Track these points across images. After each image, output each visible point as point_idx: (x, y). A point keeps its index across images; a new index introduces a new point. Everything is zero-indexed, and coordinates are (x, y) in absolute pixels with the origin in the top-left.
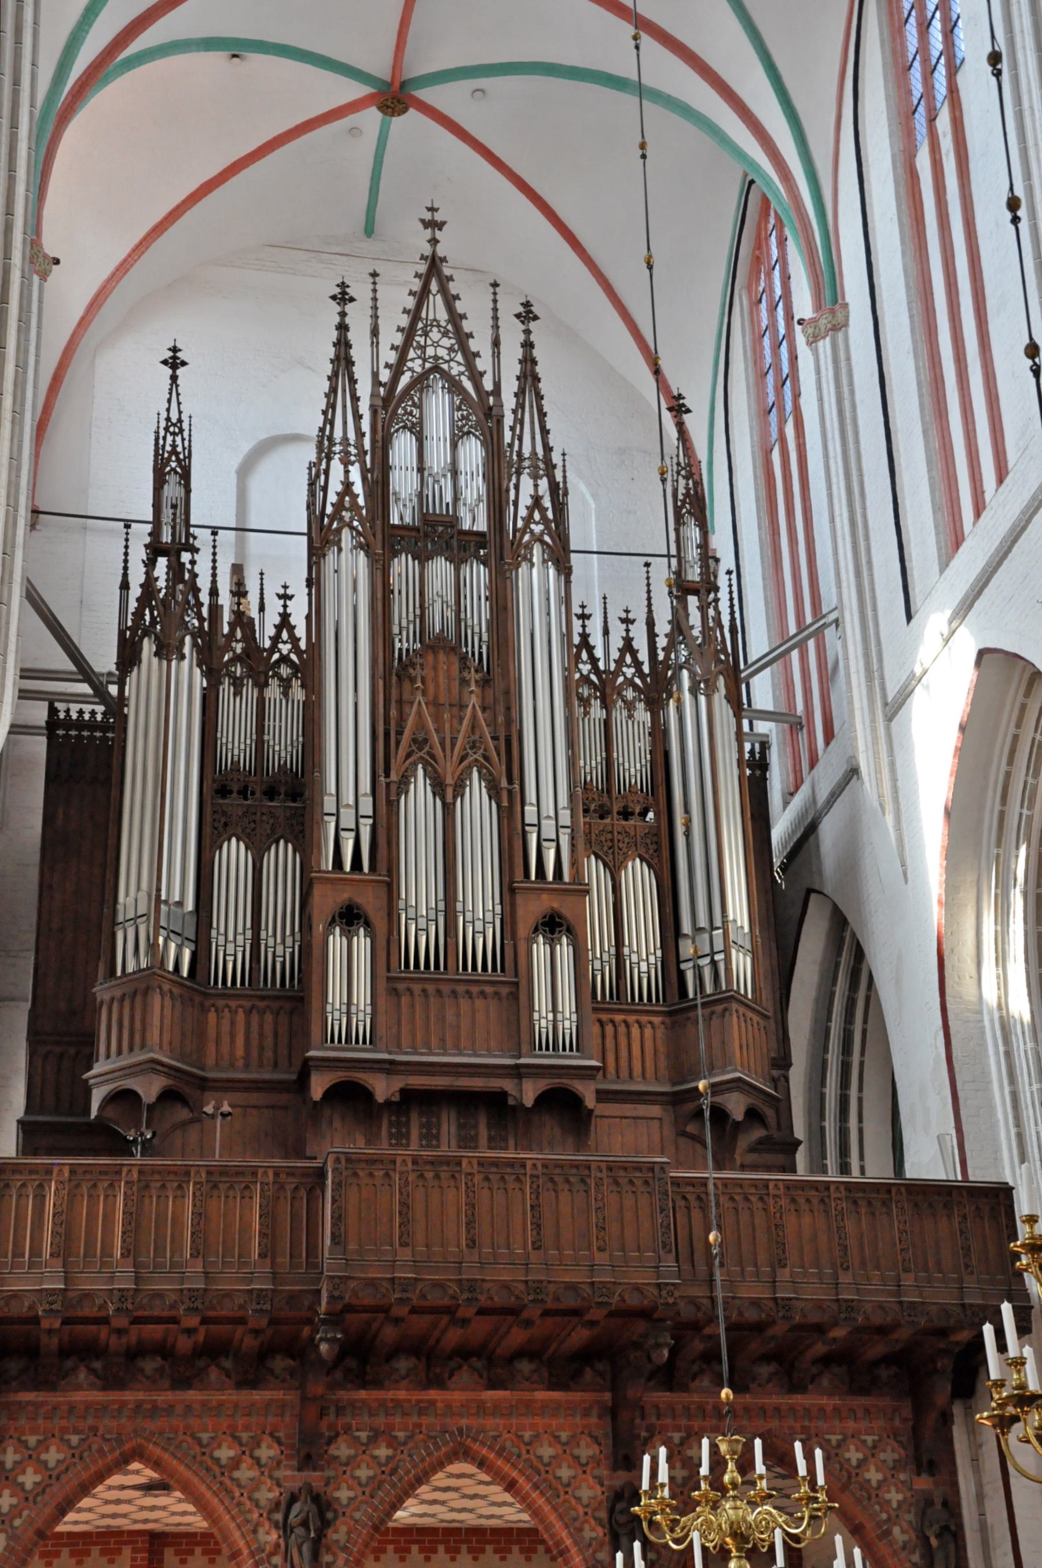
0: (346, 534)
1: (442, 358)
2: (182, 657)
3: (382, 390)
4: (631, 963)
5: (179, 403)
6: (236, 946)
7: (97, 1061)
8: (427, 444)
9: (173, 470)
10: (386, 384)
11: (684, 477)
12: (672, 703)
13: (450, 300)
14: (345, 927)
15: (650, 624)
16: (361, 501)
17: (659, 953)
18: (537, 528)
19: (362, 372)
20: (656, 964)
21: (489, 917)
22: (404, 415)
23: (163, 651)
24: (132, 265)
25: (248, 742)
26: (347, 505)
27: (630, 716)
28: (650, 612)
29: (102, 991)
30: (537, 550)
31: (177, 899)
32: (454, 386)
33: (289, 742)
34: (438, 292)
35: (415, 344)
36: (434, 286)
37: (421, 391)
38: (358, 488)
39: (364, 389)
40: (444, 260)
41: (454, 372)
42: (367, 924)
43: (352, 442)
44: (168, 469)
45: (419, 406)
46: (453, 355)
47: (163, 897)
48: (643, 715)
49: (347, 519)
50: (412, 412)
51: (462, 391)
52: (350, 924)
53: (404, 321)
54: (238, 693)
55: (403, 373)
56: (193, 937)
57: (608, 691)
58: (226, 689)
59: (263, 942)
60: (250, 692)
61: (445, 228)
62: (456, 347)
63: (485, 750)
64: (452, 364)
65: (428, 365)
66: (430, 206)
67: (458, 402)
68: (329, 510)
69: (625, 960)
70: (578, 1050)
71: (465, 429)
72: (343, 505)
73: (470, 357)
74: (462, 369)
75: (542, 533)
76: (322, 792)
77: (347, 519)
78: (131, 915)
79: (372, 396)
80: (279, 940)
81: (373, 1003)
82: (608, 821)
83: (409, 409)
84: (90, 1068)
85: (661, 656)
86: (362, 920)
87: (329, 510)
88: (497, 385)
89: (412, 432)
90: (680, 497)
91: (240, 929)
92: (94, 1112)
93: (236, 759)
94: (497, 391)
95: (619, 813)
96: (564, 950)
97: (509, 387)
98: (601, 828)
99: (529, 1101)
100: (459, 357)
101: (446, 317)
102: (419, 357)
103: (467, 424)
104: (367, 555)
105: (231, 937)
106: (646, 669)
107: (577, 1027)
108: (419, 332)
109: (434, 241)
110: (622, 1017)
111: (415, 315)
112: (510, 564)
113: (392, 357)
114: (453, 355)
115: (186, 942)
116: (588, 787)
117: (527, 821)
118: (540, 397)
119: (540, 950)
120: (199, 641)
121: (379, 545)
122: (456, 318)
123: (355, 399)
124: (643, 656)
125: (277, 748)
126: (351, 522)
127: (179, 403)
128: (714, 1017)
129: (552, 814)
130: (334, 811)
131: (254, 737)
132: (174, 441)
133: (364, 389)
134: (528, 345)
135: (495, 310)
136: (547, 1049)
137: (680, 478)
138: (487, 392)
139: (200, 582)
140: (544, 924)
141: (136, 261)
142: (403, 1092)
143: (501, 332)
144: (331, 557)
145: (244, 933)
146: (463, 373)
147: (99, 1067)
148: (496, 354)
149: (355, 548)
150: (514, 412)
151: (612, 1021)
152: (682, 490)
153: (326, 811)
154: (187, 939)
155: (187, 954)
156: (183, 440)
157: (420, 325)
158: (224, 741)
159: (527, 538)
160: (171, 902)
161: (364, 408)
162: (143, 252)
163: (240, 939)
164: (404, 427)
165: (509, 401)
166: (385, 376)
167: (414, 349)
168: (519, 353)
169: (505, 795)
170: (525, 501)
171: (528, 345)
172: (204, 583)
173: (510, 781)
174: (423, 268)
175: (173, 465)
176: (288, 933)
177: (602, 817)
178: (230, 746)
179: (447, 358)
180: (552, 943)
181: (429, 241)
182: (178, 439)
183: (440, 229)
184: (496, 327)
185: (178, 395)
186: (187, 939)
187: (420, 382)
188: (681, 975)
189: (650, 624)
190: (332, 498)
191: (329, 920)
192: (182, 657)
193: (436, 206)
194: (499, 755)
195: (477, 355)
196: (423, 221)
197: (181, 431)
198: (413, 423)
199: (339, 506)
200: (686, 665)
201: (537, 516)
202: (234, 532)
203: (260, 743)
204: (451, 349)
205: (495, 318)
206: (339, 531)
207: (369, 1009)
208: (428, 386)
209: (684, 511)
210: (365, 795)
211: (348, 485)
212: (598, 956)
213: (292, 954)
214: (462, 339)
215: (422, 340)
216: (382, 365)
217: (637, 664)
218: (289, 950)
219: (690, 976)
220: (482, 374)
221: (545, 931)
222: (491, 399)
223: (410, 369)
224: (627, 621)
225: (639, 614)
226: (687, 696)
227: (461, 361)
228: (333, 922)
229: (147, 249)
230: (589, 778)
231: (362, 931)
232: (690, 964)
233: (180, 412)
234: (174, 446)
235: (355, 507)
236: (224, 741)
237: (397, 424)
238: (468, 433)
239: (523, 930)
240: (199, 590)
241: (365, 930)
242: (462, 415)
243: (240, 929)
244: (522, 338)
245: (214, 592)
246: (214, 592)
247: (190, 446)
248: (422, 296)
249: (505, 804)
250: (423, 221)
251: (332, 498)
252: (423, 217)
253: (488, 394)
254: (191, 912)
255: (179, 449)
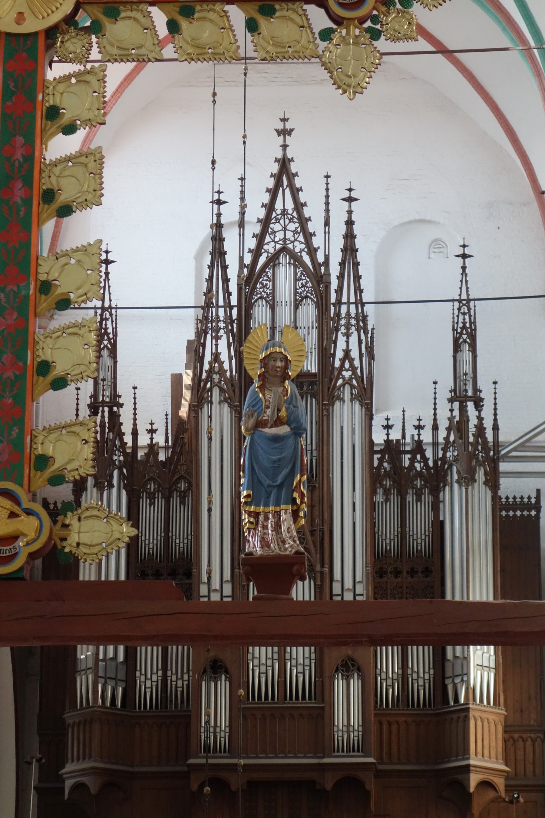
0: (216, 392)
1: (289, 240)
2: (113, 486)
3: (245, 270)
4: (412, 680)
5: (110, 294)
6: (152, 682)
7: (67, 763)
8: (277, 309)
9: (105, 346)
10: (248, 265)
11: (464, 314)
12: (447, 489)
13: (295, 192)
14: (213, 675)
15: (435, 428)
16: (226, 366)
17: (432, 672)
18: (347, 374)
19: (232, 260)
20: (429, 680)
21: (307, 662)
22: (261, 288)
23: (99, 486)
24: (112, 108)
25: (159, 538)
26: (216, 369)
27: (419, 499)
28: (435, 420)
29: (70, 717)
30: (347, 388)
31: (111, 656)
32: (296, 260)
33: (185, 537)
34: (287, 186)
35: (270, 230)
36: (285, 183)
37: (274, 266)
38: (224, 357)
39: (233, 273)
40: (292, 160)
41: (297, 250)
42: (227, 672)
43: (222, 318)
44: (102, 346)
45: (273, 280)
46: (296, 236)
47: (101, 657)
48: (427, 498)
49: (216, 380)
50: (266, 284)
51: (303, 264)
52: (215, 672)
53: (262, 213)
54: (152, 504)
55: (261, 255)
56: (124, 678)
57: (403, 482)
58: (144, 502)
59: (169, 678)
60: (160, 502)
61: (293, 133)
62: (299, 229)
63: (306, 544)
64: (296, 243)
65: (278, 246)
66: (282, 117)
67: (299, 274)
68: (204, 375)
69: (408, 678)
70: (362, 751)
71: (304, 294)
72: (214, 371)
73: (308, 237)
74: (303, 246)
75: (351, 379)
76: (199, 582)
77: (216, 380)
78: (84, 667)
79: (239, 276)
80: (179, 676)
81: (230, 726)
82: (399, 580)
83: (264, 282)
84: (64, 767)
85: (440, 454)
86: (223, 670)
87: (204, 375)
88: (327, 257)
89: (267, 301)
90: (459, 330)
91: (155, 670)
92: (66, 797)
93: (151, 552)
94: (327, 263)
95: (408, 572)
96: (355, 684)
97: (336, 257)
98: (395, 584)
99: (329, 786)
100: (301, 238)
101: (293, 206)
102: (273, 241)
103: (305, 290)
104: (230, 406)
105: (149, 676)
106: (431, 463)
107: (362, 735)
108: (273, 221)
109: (285, 147)
110: (404, 719)
111: (270, 207)
112: (326, 405)
113: (252, 243)
114: (296, 236)
115: (119, 683)
116: (387, 555)
117: (334, 593)
118: (356, 264)
119: (339, 685)
120: (125, 471)
121: (237, 399)
122: (299, 206)
123: (226, 281)
124: (429, 454)
125: (178, 541)
126: (220, 382)
127: (110, 294)
128: (460, 720)
129: (351, 587)
130: (207, 594)
131: (163, 534)
132: (106, 325)
133: (233, 273)
134: (350, 223)
135: (327, 197)
136: (343, 751)
137: (460, 314)
138: (319, 264)
139: (124, 429)
140: (342, 666)
141: (114, 104)
142: (249, 782)
143: (331, 214)
144: (206, 409)
145: (157, 673)
146: (303, 250)
147: (69, 767)
148: (327, 233)
149: (220, 402)
150: (338, 278)
151: (397, 723)
152: (460, 325)
153: (201, 594)
154: (119, 680)
155: (120, 690)
156: (112, 322)
157: (274, 215)
158: (143, 538)
159: (340, 382)
160: (108, 657)
161: (233, 287)
162: (119, 97)
163: (154, 678)
164: (261, 298)
165: (335, 270)
166: (248, 259)
167: (269, 234)
168: (343, 229)
169: (318, 576)
170: (340, 354)
171: (350, 223)
172: (127, 428)
173: (323, 566)
174: (275, 168)
175: (106, 342)
176: (185, 671)
177: (396, 577)
178: (147, 542)
179: (292, 239)
180: (347, 678)
181: (281, 146)
182: (109, 323)
183: (290, 135)
184: (327, 211)
185: (109, 287)
186: (119, 680)
187: (273, 261)
188: (445, 688)
189: (435, 428)
190: (206, 367)
191: (202, 671)
192: (113, 486)
193: (286, 117)
194: (315, 546)
195: (314, 234)
196: (277, 130)
197: (111, 315)
198: (267, 294)
199: (210, 372)
200: (456, 459)
201: (347, 365)
202: (193, 310)
203: (167, 538)
204: (295, 232)
205: (327, 204)
206: (211, 390)
207: (227, 730)
208: (279, 263)
209: (461, 340)
210: (227, 581)
211: (216, 356)
212: (391, 676)
213: (188, 685)
214: (303, 221)
215: (277, 227)
216: (246, 250)
217: (425, 460)
218: (186, 683)
219: (450, 688)
220: (316, 250)
221: (342, 670)
222: (323, 268)
223: (266, 251)
224: (419, 427)
225: (428, 423)
226: (456, 486)
227: (303, 241)
228: (205, 671)
229: (121, 94)
230: (388, 548)
231: (223, 677)
232: (451, 680)
233: (111, 301)
234: (106, 329)
235: (222, 372)
236: (143, 538)
237: (256, 296)
238: (307, 297)
239: (327, 673)
240: (124, 434)
241: (226, 676)
242: (302, 284)
243: (155, 670)
244: (345, 217)
245: (135, 433)
246: (135, 433)
247: (116, 327)
248: (274, 193)
249: (319, 583)
250: (277, 130)
251: (206, 367)
252: (277, 128)
253: (320, 265)
254: (122, 662)
255: (110, 330)
